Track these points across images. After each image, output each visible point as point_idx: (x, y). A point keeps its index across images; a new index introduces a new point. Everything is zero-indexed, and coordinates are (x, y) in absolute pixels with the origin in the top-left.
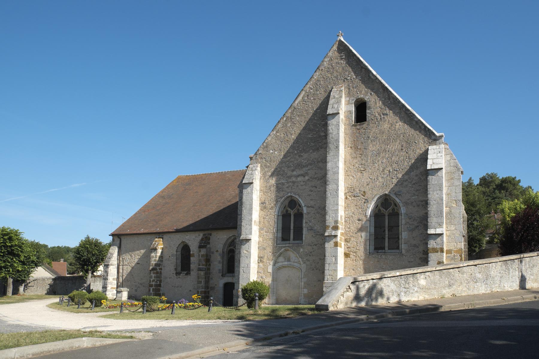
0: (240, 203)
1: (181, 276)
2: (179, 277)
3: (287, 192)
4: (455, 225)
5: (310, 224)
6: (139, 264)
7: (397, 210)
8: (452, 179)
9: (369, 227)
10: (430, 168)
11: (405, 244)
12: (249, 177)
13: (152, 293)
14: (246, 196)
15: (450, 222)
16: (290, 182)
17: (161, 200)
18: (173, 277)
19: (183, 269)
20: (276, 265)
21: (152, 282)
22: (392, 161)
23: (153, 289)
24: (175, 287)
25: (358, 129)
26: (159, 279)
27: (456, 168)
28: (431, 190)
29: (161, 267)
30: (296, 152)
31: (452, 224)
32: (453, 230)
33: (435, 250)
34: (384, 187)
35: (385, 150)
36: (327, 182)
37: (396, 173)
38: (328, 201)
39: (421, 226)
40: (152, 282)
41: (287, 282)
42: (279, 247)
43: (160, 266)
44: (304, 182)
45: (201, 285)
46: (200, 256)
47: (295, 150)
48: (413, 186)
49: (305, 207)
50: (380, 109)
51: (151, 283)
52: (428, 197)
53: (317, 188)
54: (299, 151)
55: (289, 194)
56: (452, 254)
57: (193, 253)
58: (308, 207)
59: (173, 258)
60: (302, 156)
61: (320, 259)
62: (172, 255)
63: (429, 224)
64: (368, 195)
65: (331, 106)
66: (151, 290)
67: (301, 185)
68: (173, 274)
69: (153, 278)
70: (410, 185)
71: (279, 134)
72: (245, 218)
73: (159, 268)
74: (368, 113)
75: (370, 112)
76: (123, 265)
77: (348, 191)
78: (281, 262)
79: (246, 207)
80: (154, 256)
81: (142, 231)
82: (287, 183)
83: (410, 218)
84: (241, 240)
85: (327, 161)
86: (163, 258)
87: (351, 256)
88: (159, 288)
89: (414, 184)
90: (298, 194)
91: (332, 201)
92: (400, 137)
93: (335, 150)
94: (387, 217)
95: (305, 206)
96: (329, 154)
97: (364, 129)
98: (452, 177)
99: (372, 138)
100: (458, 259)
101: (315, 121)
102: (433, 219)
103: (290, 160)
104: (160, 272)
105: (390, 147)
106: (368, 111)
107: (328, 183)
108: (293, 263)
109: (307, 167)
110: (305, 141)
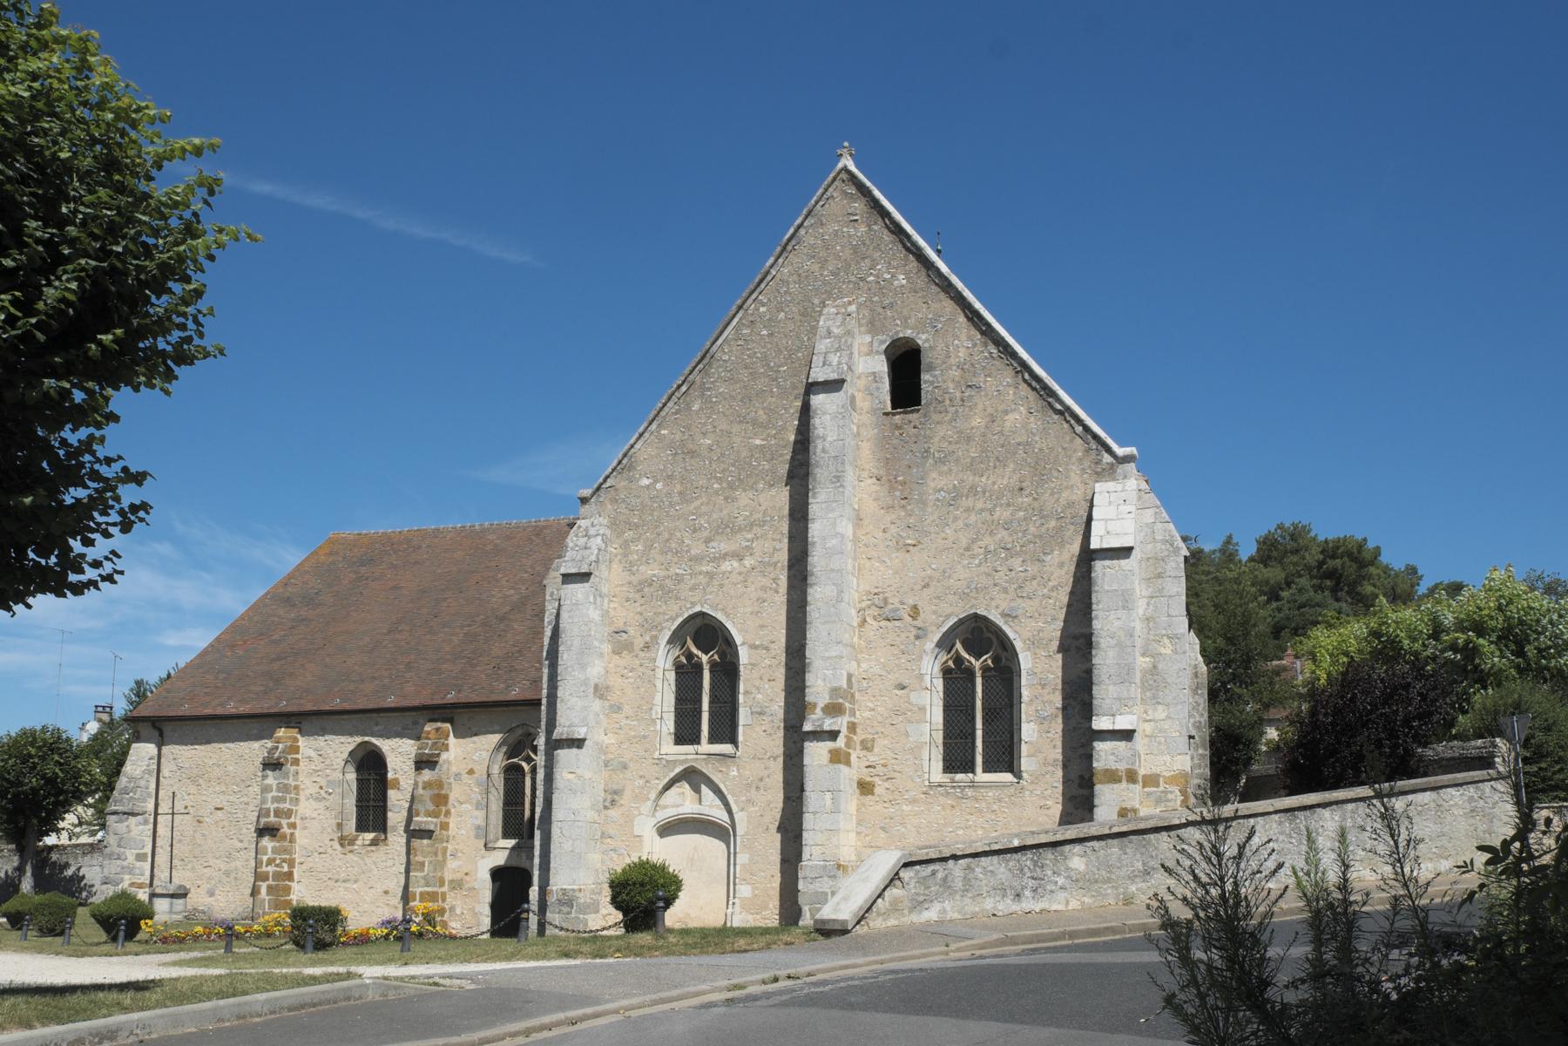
1: (356, 847)
2: (351, 851)
4: (1168, 705)
5: (760, 696)
6: (219, 812)
7: (1007, 659)
8: (1159, 576)
9: (928, 707)
10: (1098, 547)
12: (579, 557)
13: (267, 898)
15: (1154, 697)
16: (700, 573)
17: (281, 612)
18: (330, 851)
19: (362, 827)
20: (657, 814)
21: (267, 866)
22: (993, 521)
23: (270, 888)
24: (337, 881)
25: (898, 427)
26: (288, 857)
27: (1168, 546)
28: (1100, 606)
29: (292, 820)
30: (715, 486)
31: (1159, 703)
32: (1163, 720)
33: (1112, 777)
34: (971, 595)
35: (973, 490)
36: (809, 578)
37: (1003, 555)
38: (812, 631)
42: (667, 761)
43: (290, 817)
44: (740, 574)
45: (422, 874)
46: (420, 785)
50: (959, 371)
51: (264, 869)
52: (1094, 627)
54: (725, 485)
55: (697, 609)
56: (1158, 786)
58: (753, 647)
60: (734, 500)
62: (329, 781)
63: (1095, 702)
64: (927, 616)
65: (821, 359)
66: (264, 890)
67: (733, 583)
68: (331, 840)
69: (270, 855)
70: (1045, 591)
73: (287, 824)
74: (926, 382)
75: (931, 379)
76: (173, 814)
77: (869, 602)
78: (673, 807)
79: (569, 643)
81: (231, 708)
82: (690, 574)
84: (556, 740)
85: (810, 517)
86: (301, 792)
87: (877, 790)
88: (287, 882)
90: (723, 610)
91: (825, 634)
92: (1015, 453)
94: (979, 681)
95: (743, 644)
96: (814, 497)
97: (915, 427)
98: (1160, 570)
99: (936, 455)
100: (1176, 801)
101: (774, 399)
102: (1107, 689)
104: (292, 834)
105: (990, 482)
106: (925, 377)
107: (810, 580)
109: (751, 529)
110: (744, 454)
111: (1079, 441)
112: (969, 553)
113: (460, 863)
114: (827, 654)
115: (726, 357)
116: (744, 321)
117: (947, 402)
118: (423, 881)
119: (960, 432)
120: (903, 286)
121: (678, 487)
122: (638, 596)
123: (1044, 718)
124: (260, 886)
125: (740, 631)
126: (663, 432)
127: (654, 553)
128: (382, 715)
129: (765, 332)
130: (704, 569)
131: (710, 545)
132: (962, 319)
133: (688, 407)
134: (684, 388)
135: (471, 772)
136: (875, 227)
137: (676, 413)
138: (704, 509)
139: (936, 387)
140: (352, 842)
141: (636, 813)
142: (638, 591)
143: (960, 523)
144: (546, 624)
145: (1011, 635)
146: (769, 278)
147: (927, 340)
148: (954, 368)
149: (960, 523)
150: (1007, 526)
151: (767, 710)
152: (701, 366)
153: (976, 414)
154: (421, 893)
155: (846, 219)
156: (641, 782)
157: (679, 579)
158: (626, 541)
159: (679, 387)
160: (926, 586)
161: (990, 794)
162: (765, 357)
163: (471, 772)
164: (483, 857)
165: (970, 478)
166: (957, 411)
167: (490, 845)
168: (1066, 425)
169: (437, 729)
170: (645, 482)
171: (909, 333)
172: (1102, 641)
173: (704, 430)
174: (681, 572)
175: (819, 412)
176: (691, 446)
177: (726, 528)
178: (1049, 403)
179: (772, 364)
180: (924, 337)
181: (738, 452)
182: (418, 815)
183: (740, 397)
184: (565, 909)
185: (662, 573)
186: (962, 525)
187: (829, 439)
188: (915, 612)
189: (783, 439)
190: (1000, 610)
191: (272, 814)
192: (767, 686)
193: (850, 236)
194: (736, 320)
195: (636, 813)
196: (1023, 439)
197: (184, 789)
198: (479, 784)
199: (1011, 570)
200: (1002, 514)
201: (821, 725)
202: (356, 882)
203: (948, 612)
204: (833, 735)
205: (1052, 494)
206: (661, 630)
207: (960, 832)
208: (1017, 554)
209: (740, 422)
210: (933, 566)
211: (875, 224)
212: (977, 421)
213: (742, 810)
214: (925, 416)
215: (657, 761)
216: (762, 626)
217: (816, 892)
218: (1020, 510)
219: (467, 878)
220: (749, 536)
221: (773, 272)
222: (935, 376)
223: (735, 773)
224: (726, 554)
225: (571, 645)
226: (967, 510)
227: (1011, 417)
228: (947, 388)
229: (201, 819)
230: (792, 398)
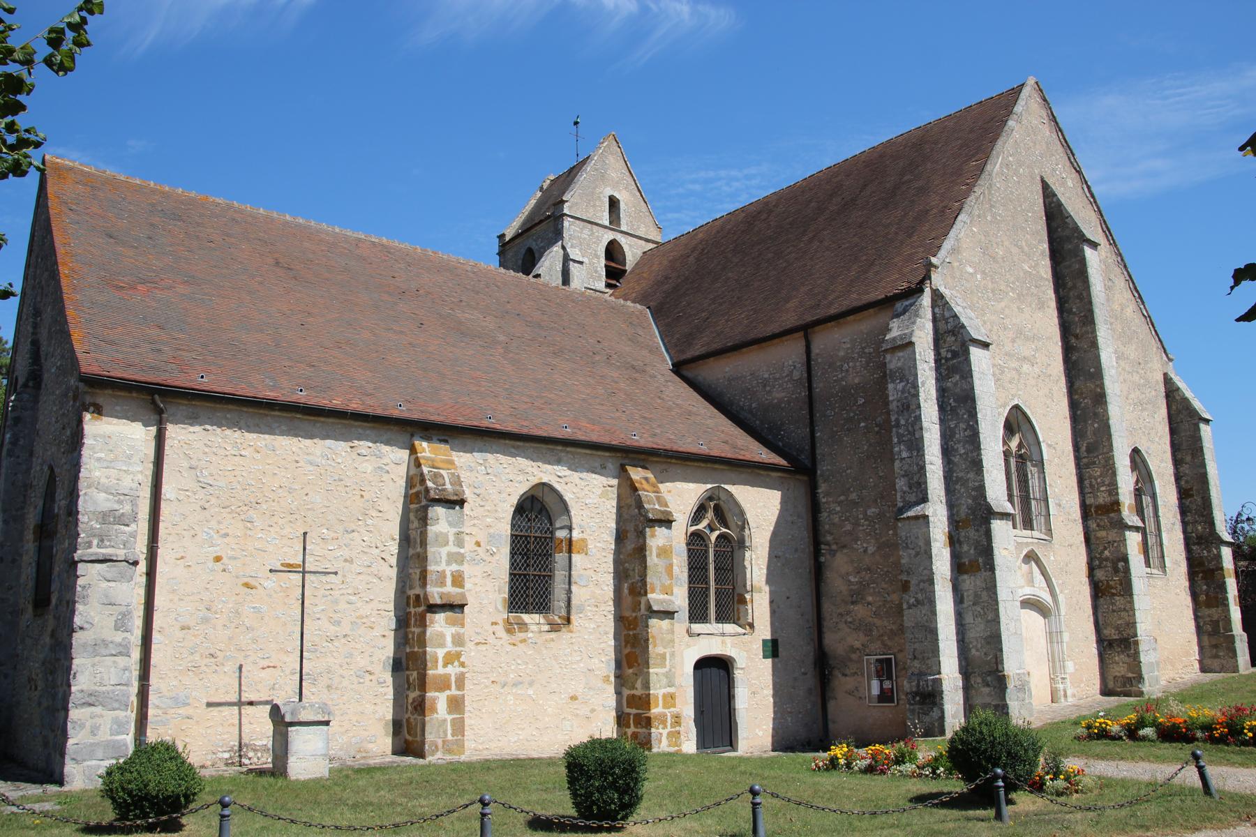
1: (530, 635)
2: (523, 641)
13: (449, 717)
18: (491, 639)
21: (445, 665)
40: (445, 665)
45: (664, 670)
68: (493, 624)
69: (450, 647)
76: (304, 572)
80: (446, 535)
95: (1044, 441)
124: (434, 700)
128: (568, 449)
144: (920, 385)
154: (665, 696)
164: (688, 646)
170: (971, 270)
182: (653, 591)
191: (449, 580)
202: (531, 684)
229: (253, 582)
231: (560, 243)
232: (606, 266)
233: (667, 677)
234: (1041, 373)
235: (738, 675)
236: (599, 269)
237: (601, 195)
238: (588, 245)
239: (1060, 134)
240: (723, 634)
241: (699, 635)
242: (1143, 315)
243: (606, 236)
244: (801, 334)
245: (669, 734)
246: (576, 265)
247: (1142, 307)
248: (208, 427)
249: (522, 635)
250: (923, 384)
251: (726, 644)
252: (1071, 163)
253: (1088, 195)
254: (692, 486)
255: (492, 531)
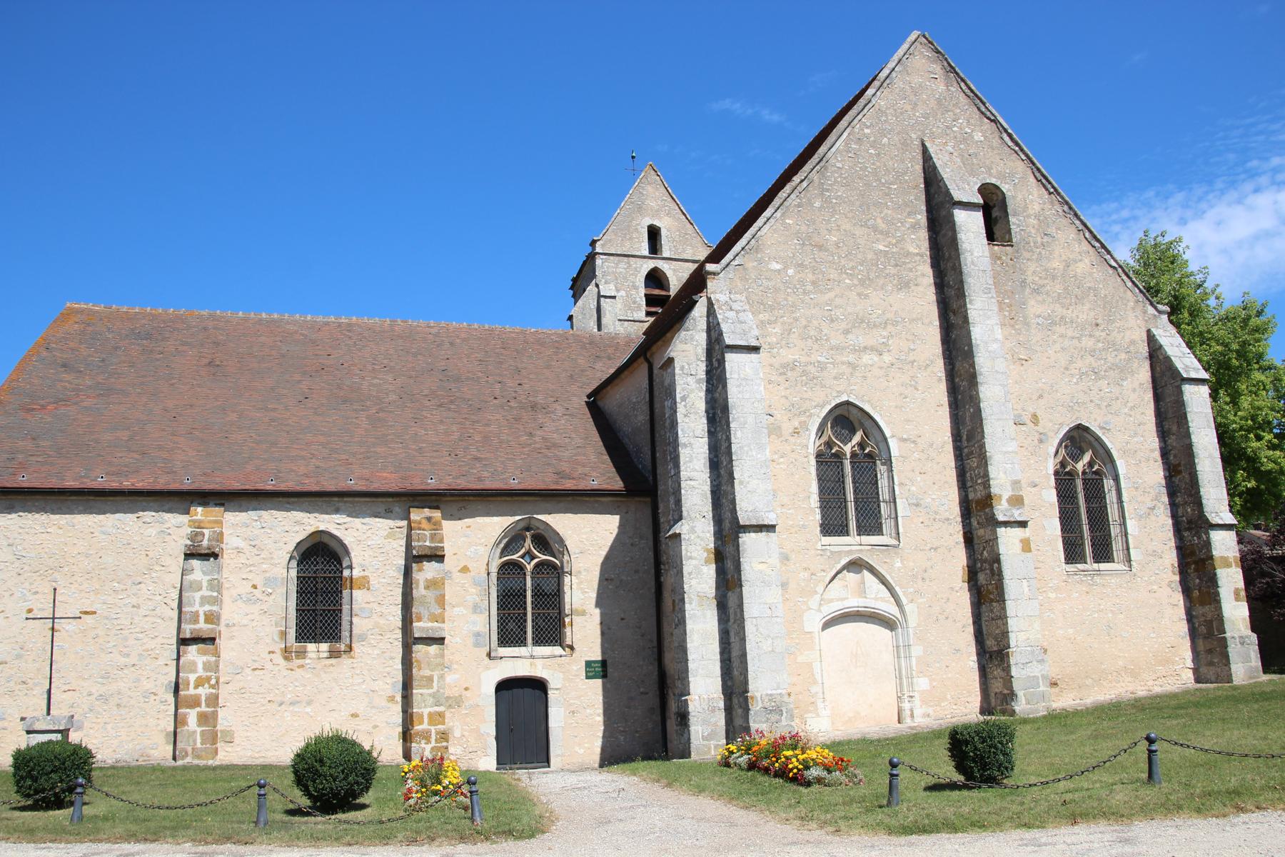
0: (685, 406)
1: (308, 661)
3: (838, 392)
5: (913, 488)
11: (1134, 548)
14: (739, 386)
16: (843, 363)
18: (269, 666)
24: (281, 705)
30: (847, 281)
37: (1093, 377)
39: (1159, 508)
41: (854, 661)
42: (831, 552)
44: (881, 368)
45: (430, 691)
47: (844, 276)
48: (1132, 413)
49: (894, 439)
53: (918, 390)
54: (856, 282)
55: (844, 398)
57: (362, 574)
59: (270, 591)
60: (867, 296)
61: (952, 589)
64: (1045, 424)
67: (875, 377)
68: (270, 653)
70: (1126, 410)
71: (791, 222)
72: (744, 457)
78: (838, 600)
80: (200, 582)
83: (1137, 488)
86: (225, 592)
89: (1132, 408)
90: (869, 401)
91: (1000, 430)
92: (1088, 295)
93: (986, 296)
96: (970, 303)
101: (889, 212)
103: (831, 300)
108: (873, 601)
111: (1129, 293)
112: (1069, 372)
113: (457, 676)
114: (1004, 449)
115: (839, 165)
116: (851, 137)
117: (1032, 244)
118: (431, 700)
119: (1046, 270)
120: (981, 141)
121: (810, 277)
122: (781, 379)
123: (1141, 516)
125: (888, 423)
126: (787, 221)
127: (794, 338)
128: (345, 499)
129: (872, 151)
130: (845, 359)
131: (850, 336)
132: (1032, 180)
133: (810, 203)
134: (805, 184)
135: (465, 569)
136: (952, 89)
137: (799, 206)
138: (838, 301)
139: (1022, 230)
140: (302, 654)
141: (804, 607)
142: (781, 374)
143: (1057, 347)
145: (1109, 445)
146: (870, 105)
147: (1009, 190)
148: (1033, 217)
149: (1057, 347)
150: (1092, 352)
151: (922, 502)
152: (818, 167)
153: (1054, 258)
154: (430, 715)
155: (927, 75)
156: (806, 574)
157: (822, 366)
158: (762, 322)
159: (802, 181)
160: (1041, 397)
161: (1113, 581)
162: (875, 173)
163: (465, 569)
164: (487, 668)
165: (1060, 311)
166: (1040, 253)
167: (493, 654)
168: (1119, 280)
169: (429, 519)
170: (776, 266)
171: (993, 181)
172: (1200, 452)
173: (829, 227)
174: (822, 359)
175: (963, 228)
176: (817, 239)
177: (861, 322)
178: (1105, 260)
179: (883, 181)
180: (1007, 186)
181: (864, 252)
182: (419, 620)
183: (858, 203)
184: (774, 717)
185: (803, 359)
186: (1059, 349)
187: (976, 254)
188: (1035, 419)
189: (903, 249)
190: (1097, 423)
191: (202, 618)
192: (919, 479)
193: (933, 90)
194: (845, 134)
195: (804, 607)
196: (1092, 285)
197: (27, 585)
198: (476, 583)
199: (1101, 390)
200: (1088, 343)
201: (1012, 516)
202: (309, 703)
203: (1060, 421)
204: (1023, 524)
205: (1119, 332)
206: (811, 416)
207: (1096, 615)
208: (1104, 377)
209: (862, 226)
210: (1043, 380)
211: (952, 86)
212: (1056, 264)
213: (912, 601)
214: (1017, 252)
215: (821, 553)
216: (908, 421)
217: (1029, 677)
218: (1099, 341)
219: (468, 694)
220: (885, 333)
221: (873, 102)
222: (1020, 221)
223: (898, 564)
224: (865, 348)
225: (745, 423)
226: (1061, 336)
227: (1081, 265)
228: (1030, 232)
230: (905, 214)
231: (594, 282)
232: (646, 295)
233: (434, 697)
234: (894, 361)
235: (552, 695)
236: (638, 299)
237: (639, 227)
238: (625, 278)
239: (962, 85)
240: (532, 657)
241: (501, 658)
242: (1111, 266)
243: (645, 266)
244: (641, 360)
245: (432, 748)
246: (608, 300)
247: (1108, 257)
248: (21, 514)
249: (300, 662)
250: (684, 398)
251: (536, 666)
252: (982, 113)
253: (1010, 143)
254: (496, 519)
255: (268, 575)
